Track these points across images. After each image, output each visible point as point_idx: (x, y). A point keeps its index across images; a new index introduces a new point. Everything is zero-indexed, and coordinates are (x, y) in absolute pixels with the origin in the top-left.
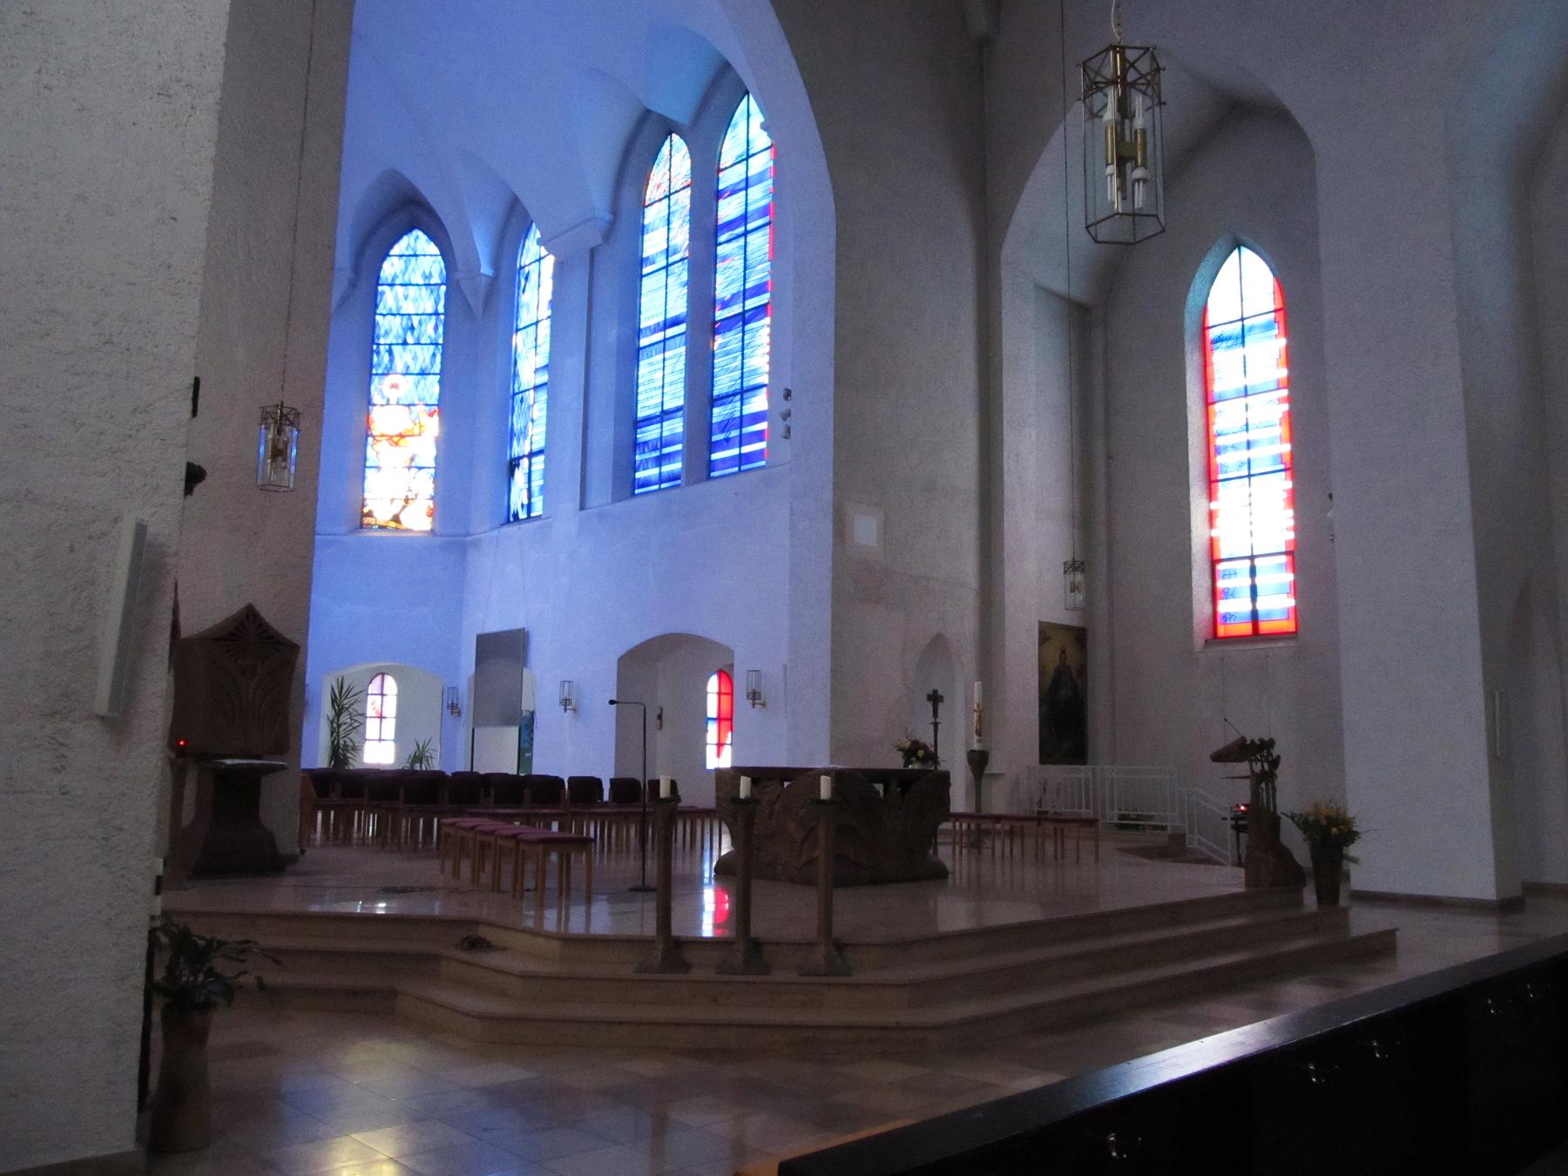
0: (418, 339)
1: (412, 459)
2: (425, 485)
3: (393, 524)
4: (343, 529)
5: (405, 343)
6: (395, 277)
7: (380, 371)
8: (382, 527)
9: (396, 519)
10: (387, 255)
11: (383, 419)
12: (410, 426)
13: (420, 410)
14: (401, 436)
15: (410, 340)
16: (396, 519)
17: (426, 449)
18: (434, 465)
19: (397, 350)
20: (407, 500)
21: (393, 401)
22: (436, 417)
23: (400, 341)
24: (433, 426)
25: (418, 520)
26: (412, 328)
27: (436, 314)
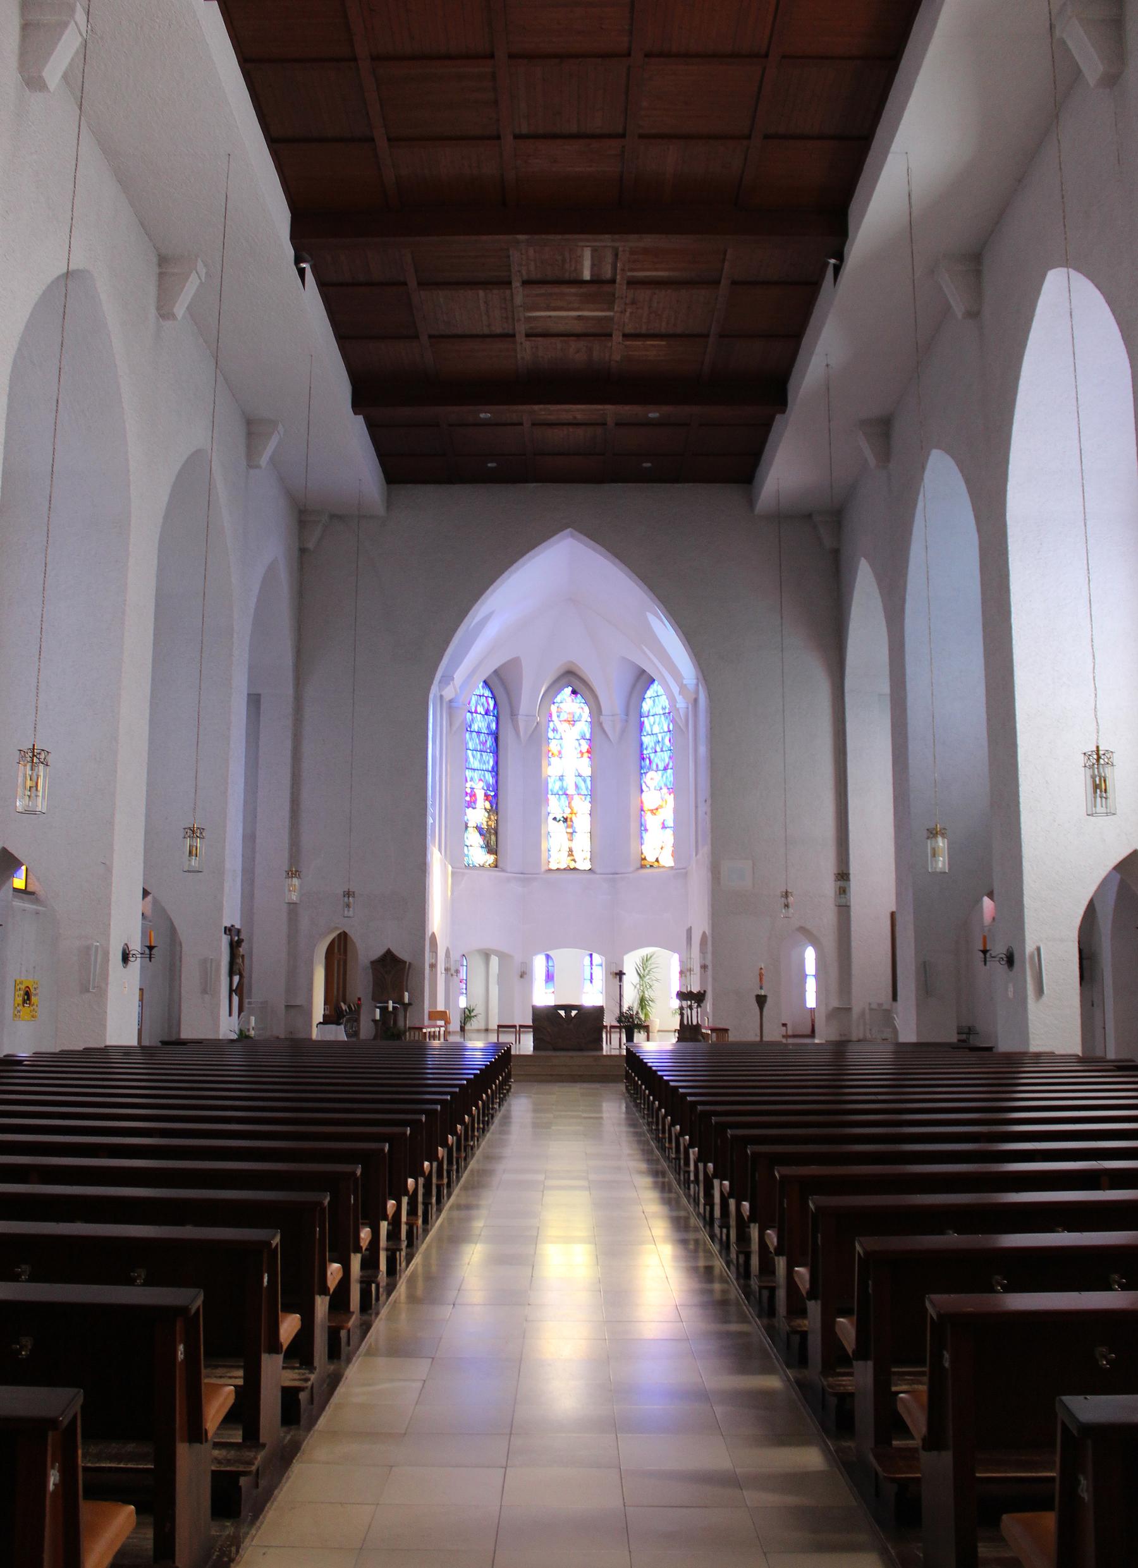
0: (662, 748)
1: (663, 824)
2: (668, 837)
3: (656, 864)
4: (632, 869)
5: (656, 752)
6: (649, 712)
7: (645, 771)
8: (651, 866)
9: (657, 860)
10: (644, 698)
11: (650, 799)
12: (661, 803)
13: (665, 790)
14: (657, 809)
15: (658, 749)
16: (657, 860)
17: (667, 814)
18: (673, 826)
19: (652, 756)
20: (662, 848)
21: (652, 788)
22: (672, 795)
23: (654, 751)
24: (670, 799)
25: (667, 861)
26: (659, 742)
27: (669, 731)
